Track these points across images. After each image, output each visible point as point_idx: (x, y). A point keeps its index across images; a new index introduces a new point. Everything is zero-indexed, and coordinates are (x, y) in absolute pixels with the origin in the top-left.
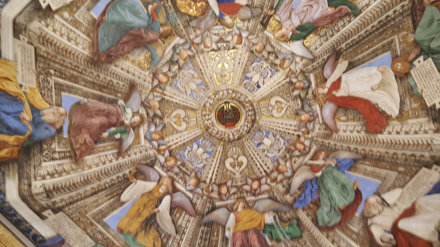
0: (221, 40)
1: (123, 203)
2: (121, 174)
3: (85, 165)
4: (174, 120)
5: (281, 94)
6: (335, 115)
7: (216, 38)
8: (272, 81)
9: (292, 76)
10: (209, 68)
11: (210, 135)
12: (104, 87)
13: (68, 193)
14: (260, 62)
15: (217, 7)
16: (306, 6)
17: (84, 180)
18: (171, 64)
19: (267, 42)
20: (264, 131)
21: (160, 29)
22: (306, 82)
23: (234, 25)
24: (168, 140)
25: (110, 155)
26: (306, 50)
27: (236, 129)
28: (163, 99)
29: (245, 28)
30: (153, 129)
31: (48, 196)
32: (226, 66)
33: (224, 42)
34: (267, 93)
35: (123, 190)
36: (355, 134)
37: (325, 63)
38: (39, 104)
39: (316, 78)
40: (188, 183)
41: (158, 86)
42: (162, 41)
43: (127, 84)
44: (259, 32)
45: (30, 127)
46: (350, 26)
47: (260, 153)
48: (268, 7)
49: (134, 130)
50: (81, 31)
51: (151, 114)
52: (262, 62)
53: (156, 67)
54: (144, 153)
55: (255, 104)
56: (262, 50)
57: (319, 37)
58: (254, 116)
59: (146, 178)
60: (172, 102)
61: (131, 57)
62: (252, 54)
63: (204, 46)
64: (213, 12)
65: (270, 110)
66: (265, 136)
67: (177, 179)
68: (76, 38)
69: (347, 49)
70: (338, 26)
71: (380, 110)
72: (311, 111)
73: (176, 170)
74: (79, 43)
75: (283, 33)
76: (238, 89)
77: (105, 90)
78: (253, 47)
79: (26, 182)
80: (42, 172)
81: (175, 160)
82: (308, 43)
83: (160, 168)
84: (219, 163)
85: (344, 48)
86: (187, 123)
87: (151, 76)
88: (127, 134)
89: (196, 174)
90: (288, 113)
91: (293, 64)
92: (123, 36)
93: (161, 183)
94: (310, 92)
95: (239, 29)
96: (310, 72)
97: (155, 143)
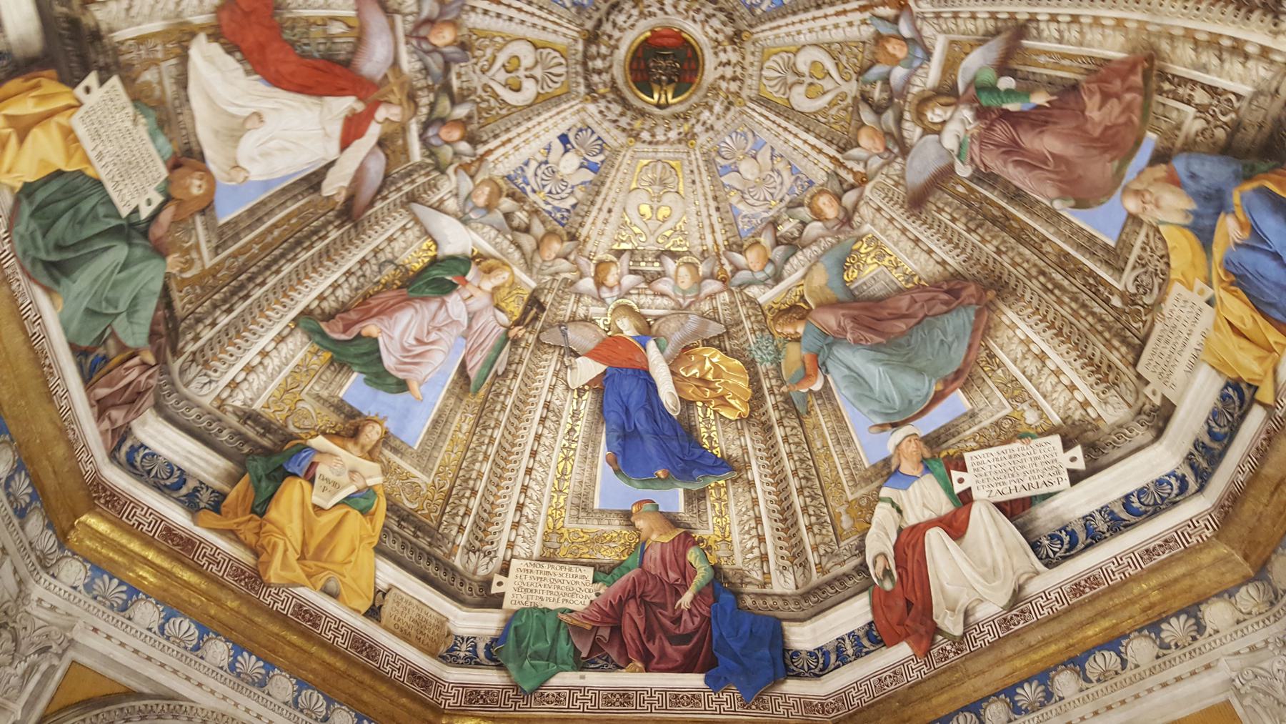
0: (650, 279)
5: (504, 112)
7: (663, 285)
8: (525, 153)
9: (467, 160)
10: (693, 209)
12: (994, 221)
14: (554, 207)
15: (650, 360)
16: (432, 343)
18: (795, 239)
19: (532, 259)
21: (804, 333)
22: (434, 141)
23: (614, 310)
24: (864, 28)
26: (431, 230)
27: (651, 22)
28: (842, 150)
29: (586, 300)
30: (898, 74)
32: (645, 209)
33: (643, 273)
34: (541, 118)
37: (379, 191)
39: (405, 150)
41: (845, 186)
42: (806, 302)
43: (929, 212)
48: (523, 345)
49: (955, 86)
51: (889, 116)
52: (549, 208)
53: (839, 241)
54: (947, 11)
55: (582, 89)
56: (546, 240)
57: (396, 262)
58: (589, 54)
60: (818, 136)
61: (897, 277)
62: (573, 230)
63: (697, 268)
64: (662, 351)
68: (1024, 358)
69: (325, 225)
70: (350, 285)
71: (238, 55)
72: (427, 52)
74: (1022, 341)
75: (489, 278)
76: (622, 138)
77: (997, 213)
78: (568, 250)
82: (424, 247)
85: (331, 227)
87: (856, 218)
88: (978, 79)
90: (489, 52)
91: (464, 193)
92: (903, 333)
94: (425, 110)
95: (602, 300)
96: (420, 166)
97: (905, 29)
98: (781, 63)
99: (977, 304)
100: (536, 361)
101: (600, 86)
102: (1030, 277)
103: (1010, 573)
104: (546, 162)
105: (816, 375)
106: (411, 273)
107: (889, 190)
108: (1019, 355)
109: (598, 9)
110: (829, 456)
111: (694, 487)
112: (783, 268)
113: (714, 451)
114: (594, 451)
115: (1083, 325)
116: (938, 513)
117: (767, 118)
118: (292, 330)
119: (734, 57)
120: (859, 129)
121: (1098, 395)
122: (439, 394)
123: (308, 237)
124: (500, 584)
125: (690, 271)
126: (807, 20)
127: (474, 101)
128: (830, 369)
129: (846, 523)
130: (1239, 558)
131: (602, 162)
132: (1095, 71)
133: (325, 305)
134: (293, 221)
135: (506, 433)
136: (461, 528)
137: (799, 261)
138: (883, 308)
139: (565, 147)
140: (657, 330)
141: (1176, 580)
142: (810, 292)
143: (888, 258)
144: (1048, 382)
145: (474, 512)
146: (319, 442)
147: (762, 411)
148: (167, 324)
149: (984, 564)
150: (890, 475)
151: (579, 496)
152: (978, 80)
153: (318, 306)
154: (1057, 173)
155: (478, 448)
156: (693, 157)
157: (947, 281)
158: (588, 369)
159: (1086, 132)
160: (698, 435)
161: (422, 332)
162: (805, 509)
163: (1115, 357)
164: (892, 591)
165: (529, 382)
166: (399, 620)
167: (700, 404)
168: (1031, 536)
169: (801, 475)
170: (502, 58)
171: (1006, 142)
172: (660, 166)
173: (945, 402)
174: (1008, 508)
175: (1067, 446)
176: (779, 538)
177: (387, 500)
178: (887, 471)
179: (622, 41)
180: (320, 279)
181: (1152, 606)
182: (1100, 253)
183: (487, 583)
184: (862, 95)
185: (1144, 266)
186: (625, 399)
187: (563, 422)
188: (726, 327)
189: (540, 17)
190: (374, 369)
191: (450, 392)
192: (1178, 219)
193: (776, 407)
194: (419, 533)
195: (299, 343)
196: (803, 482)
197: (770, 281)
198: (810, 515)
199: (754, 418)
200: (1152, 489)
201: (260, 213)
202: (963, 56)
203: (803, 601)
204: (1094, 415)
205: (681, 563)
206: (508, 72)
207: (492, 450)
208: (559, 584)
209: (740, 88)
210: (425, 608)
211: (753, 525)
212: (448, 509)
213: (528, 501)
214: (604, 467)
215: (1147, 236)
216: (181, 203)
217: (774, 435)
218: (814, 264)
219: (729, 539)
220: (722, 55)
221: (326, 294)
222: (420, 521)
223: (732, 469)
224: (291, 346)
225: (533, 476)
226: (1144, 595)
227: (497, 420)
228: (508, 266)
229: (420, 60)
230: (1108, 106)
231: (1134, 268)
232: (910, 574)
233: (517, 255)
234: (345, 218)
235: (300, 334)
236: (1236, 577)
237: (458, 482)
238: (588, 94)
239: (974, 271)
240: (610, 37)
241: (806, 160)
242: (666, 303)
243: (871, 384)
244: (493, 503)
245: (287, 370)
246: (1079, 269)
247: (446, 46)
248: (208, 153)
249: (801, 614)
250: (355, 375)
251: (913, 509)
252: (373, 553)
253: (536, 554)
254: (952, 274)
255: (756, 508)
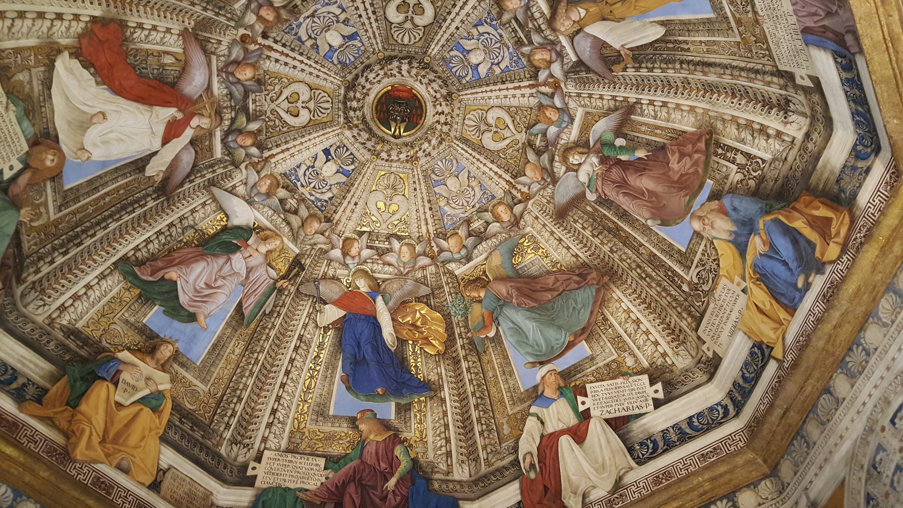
0: (381, 253)
1: (663, 23)
2: (644, 72)
3: (699, 118)
4: (507, 133)
5: (285, 129)
6: (184, 67)
7: (389, 258)
8: (298, 158)
9: (256, 160)
10: (414, 208)
11: (445, 83)
12: (610, 231)
13: (751, 88)
15: (378, 310)
16: (218, 287)
17: (713, 93)
18: (481, 233)
20: (336, 62)
22: (232, 145)
24: (531, 99)
25: (648, 116)
26: (225, 206)
28: (515, 177)
31: (788, 102)
32: (381, 205)
33: (377, 249)
34: (311, 137)
35: (651, 44)
36: (148, 23)
37: (188, 176)
38: (729, 251)
39: (211, 149)
40: (523, 4)
41: (515, 201)
42: (487, 276)
43: (568, 222)
44: (308, 253)
45: (761, 226)
46: (138, 239)
47: (354, 19)
48: (286, 293)
50: (614, 330)
51: (545, 157)
52: (312, 198)
54: (585, 93)
55: (342, 120)
56: (309, 221)
59: (601, 46)
60: (499, 167)
62: (329, 215)
63: (415, 248)
64: (386, 304)
65: (312, 101)
66: (336, 50)
67: (541, 21)
68: (626, 322)
71: (92, 70)
72: (232, 83)
73: (536, 38)
74: (625, 311)
75: (265, 244)
76: (368, 155)
78: (325, 229)
79: (810, 146)
80: (777, 147)
81: (532, 58)
82: (218, 218)
83: (568, 54)
84: (445, 20)
85: (150, 198)
86: (484, 120)
87: (522, 223)
88: (603, 138)
89: (500, 15)
90: (277, 88)
91: (251, 182)
92: (549, 301)
93: (576, 25)
94: (227, 123)
95: (346, 266)
96: (220, 161)
97: (558, 102)
98: (477, 115)
99: (597, 285)
100: (295, 305)
101: (354, 119)
102: (631, 269)
103: (614, 468)
104: (313, 167)
105: (491, 325)
106: (206, 236)
107: (544, 206)
108: (623, 320)
109: (356, 68)
110: (497, 383)
111: (403, 401)
112: (473, 252)
113: (419, 376)
114: (333, 372)
115: (664, 302)
116: (568, 425)
117: (466, 152)
118: (112, 271)
119: (447, 110)
120: (526, 164)
121: (672, 349)
122: (220, 325)
123: (131, 204)
124: (254, 468)
125: (409, 249)
126: (495, 90)
127: (264, 120)
128: (501, 322)
129: (506, 430)
130: (760, 461)
131: (353, 170)
132: (676, 139)
133: (139, 254)
134: (122, 191)
135: (268, 357)
136: (228, 426)
137: (484, 248)
138: (536, 283)
139: (327, 157)
140: (384, 289)
141: (721, 475)
142: (490, 269)
143: (541, 250)
144: (641, 340)
145: (238, 414)
146: (125, 355)
147: (453, 349)
148: (15, 260)
149: (597, 462)
150: (537, 397)
151: (319, 405)
152: (603, 138)
153: (134, 254)
154: (650, 202)
155: (246, 367)
156: (416, 172)
157: (579, 268)
158: (332, 313)
159: (669, 177)
160: (408, 364)
161: (211, 279)
162: (479, 420)
163: (684, 324)
164: (536, 479)
165: (288, 320)
166: (174, 492)
167: (411, 342)
168: (628, 443)
169: (478, 396)
170: (286, 93)
171: (619, 180)
172: (392, 176)
173: (575, 348)
174: (613, 423)
175: (652, 382)
176: (460, 440)
177: (173, 401)
178: (535, 395)
179: (372, 90)
180: (137, 236)
181: (705, 493)
182: (676, 256)
183: (245, 467)
184: (528, 142)
185: (703, 265)
186: (358, 336)
187: (311, 350)
188: (432, 290)
189: (315, 68)
190: (172, 304)
191: (228, 324)
192: (725, 236)
193: (463, 347)
194: (195, 428)
195: (116, 281)
196: (479, 400)
197: (463, 260)
198: (482, 424)
199: (448, 354)
200: (706, 413)
201: (97, 184)
202: (594, 122)
203: (474, 486)
204: (670, 363)
205: (390, 455)
206: (289, 102)
207: (256, 369)
208: (299, 470)
209: (450, 130)
210: (196, 484)
211: (443, 430)
212: (219, 411)
213: (280, 407)
214: (339, 384)
215: (706, 246)
216: (36, 171)
217: (460, 368)
218: (493, 251)
219: (425, 440)
220: (438, 107)
221: (140, 247)
222: (197, 418)
223: (430, 389)
224: (110, 282)
225: (286, 389)
226: (700, 485)
227: (262, 346)
228: (280, 236)
229: (227, 88)
230: (684, 161)
231: (697, 266)
232: (548, 469)
233: (287, 229)
234: (160, 193)
235: (117, 274)
236: (758, 474)
237: (229, 391)
238: (346, 124)
239: (596, 262)
240: (364, 87)
241: (490, 181)
242: (392, 270)
243: (527, 333)
244: (253, 408)
245: (105, 300)
246: (662, 265)
247: (246, 80)
248: (61, 136)
249: (473, 495)
250: (157, 307)
251: (551, 421)
252: (158, 441)
253: (283, 447)
254: (582, 264)
255: (445, 418)
